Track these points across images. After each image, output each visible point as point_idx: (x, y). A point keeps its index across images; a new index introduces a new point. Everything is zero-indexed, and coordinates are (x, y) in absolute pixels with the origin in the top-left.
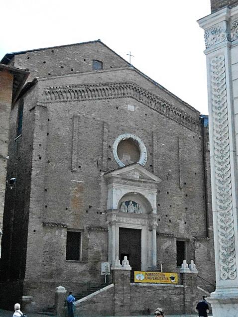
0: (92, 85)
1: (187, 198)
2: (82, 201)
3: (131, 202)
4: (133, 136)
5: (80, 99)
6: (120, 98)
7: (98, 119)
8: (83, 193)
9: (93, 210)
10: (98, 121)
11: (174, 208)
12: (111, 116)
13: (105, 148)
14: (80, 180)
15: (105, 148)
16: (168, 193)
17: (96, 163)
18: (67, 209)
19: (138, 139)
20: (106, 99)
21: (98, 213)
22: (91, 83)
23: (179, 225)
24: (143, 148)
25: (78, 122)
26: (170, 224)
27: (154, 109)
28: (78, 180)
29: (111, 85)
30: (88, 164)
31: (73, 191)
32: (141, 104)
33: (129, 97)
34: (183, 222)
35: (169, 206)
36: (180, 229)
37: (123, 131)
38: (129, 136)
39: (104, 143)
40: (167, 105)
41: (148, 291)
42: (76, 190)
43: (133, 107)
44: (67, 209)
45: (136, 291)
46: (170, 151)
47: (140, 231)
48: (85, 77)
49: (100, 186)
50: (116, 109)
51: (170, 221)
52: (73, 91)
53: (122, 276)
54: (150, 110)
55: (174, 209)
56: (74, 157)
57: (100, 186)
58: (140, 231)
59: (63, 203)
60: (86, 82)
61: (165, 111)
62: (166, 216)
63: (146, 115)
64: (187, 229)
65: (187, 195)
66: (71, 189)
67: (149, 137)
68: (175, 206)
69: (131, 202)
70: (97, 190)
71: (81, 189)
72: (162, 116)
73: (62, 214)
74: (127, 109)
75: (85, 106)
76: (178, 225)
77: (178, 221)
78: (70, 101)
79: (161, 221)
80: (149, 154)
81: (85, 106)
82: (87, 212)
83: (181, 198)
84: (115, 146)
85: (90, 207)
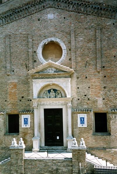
0: (17, 8)
1: (105, 79)
2: (17, 94)
3: (52, 90)
4: (53, 39)
5: (9, 21)
6: (40, 11)
7: (25, 33)
8: (17, 88)
9: (25, 99)
10: (24, 34)
11: (92, 88)
12: (34, 28)
13: (31, 54)
14: (14, 80)
15: (31, 54)
16: (86, 77)
17: (25, 66)
18: (6, 101)
19: (58, 40)
20: (29, 15)
21: (28, 100)
22: (16, 6)
23: (97, 102)
24: (63, 46)
25: (8, 40)
26: (89, 102)
27: (72, 11)
28: (13, 80)
29: (32, 2)
30: (19, 68)
31: (10, 88)
32: (59, 10)
33: (48, 8)
34: (101, 99)
35: (87, 88)
36: (98, 104)
37: (45, 37)
38: (50, 39)
39: (29, 50)
40: (84, 3)
41: (39, 164)
42: (12, 87)
43: (53, 15)
44: (6, 101)
45: (28, 164)
46: (88, 43)
47: (61, 109)
48: (12, 3)
49: (29, 81)
50: (38, 21)
51: (89, 99)
52: (3, 18)
53: (17, 153)
54: (69, 13)
55: (92, 89)
56: (8, 65)
57: (29, 81)
58: (61, 109)
59: (3, 98)
60: (12, 7)
61: (82, 9)
62: (85, 95)
63: (65, 18)
64: (106, 104)
65: (105, 76)
66: (8, 87)
67: (67, 36)
68: (94, 87)
69: (52, 90)
70: (27, 85)
71: (15, 86)
72: (80, 14)
73: (3, 104)
74: (47, 18)
75: (13, 26)
76: (96, 101)
77: (97, 98)
78: (2, 26)
79: (80, 100)
80: (68, 50)
81: (13, 26)
82: (20, 101)
83: (100, 80)
84: (40, 51)
85: (23, 97)
